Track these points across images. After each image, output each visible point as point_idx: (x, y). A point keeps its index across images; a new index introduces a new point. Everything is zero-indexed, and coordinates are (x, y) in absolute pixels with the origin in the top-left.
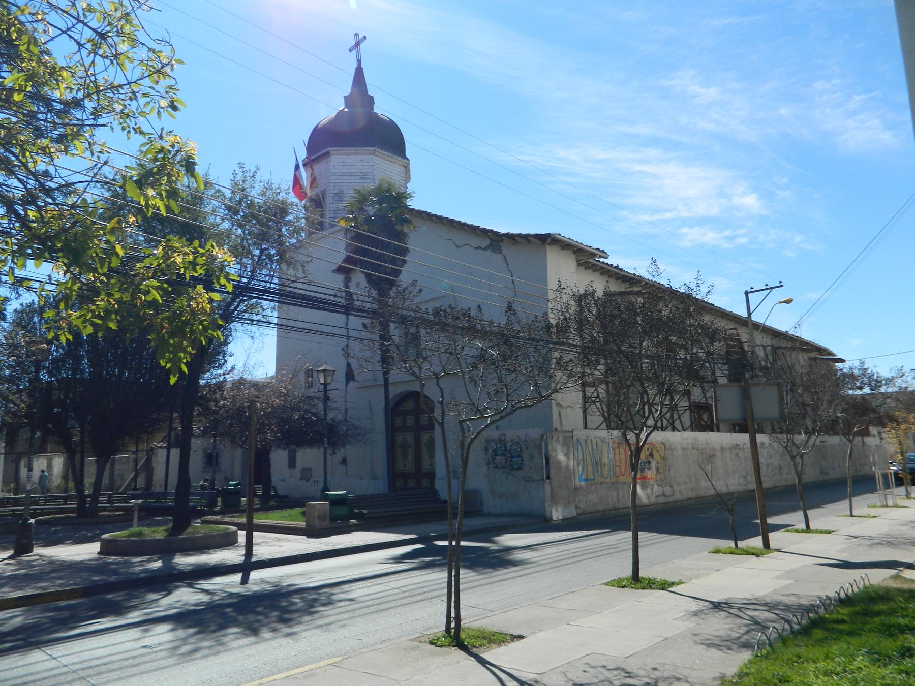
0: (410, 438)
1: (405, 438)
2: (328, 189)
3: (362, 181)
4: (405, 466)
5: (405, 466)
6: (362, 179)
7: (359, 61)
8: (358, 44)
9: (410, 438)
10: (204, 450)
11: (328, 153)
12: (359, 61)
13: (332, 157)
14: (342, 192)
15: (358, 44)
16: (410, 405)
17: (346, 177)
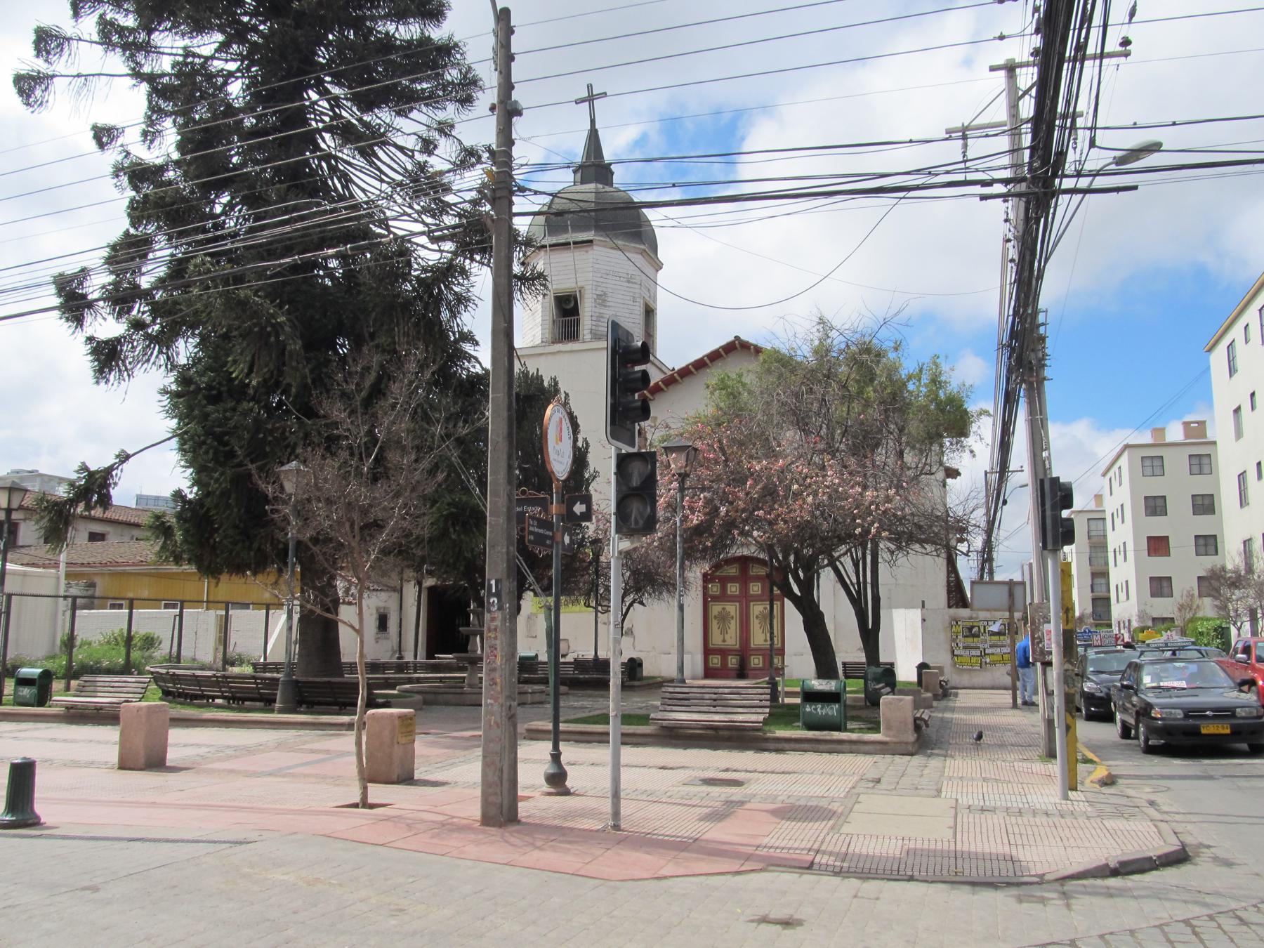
0: (732, 609)
1: (724, 609)
2: (586, 287)
3: (627, 284)
4: (724, 641)
5: (724, 641)
6: (629, 282)
7: (593, 122)
8: (591, 99)
9: (732, 609)
10: (378, 609)
11: (591, 241)
12: (593, 122)
13: (595, 247)
14: (605, 294)
15: (591, 99)
16: (733, 571)
17: (610, 277)
